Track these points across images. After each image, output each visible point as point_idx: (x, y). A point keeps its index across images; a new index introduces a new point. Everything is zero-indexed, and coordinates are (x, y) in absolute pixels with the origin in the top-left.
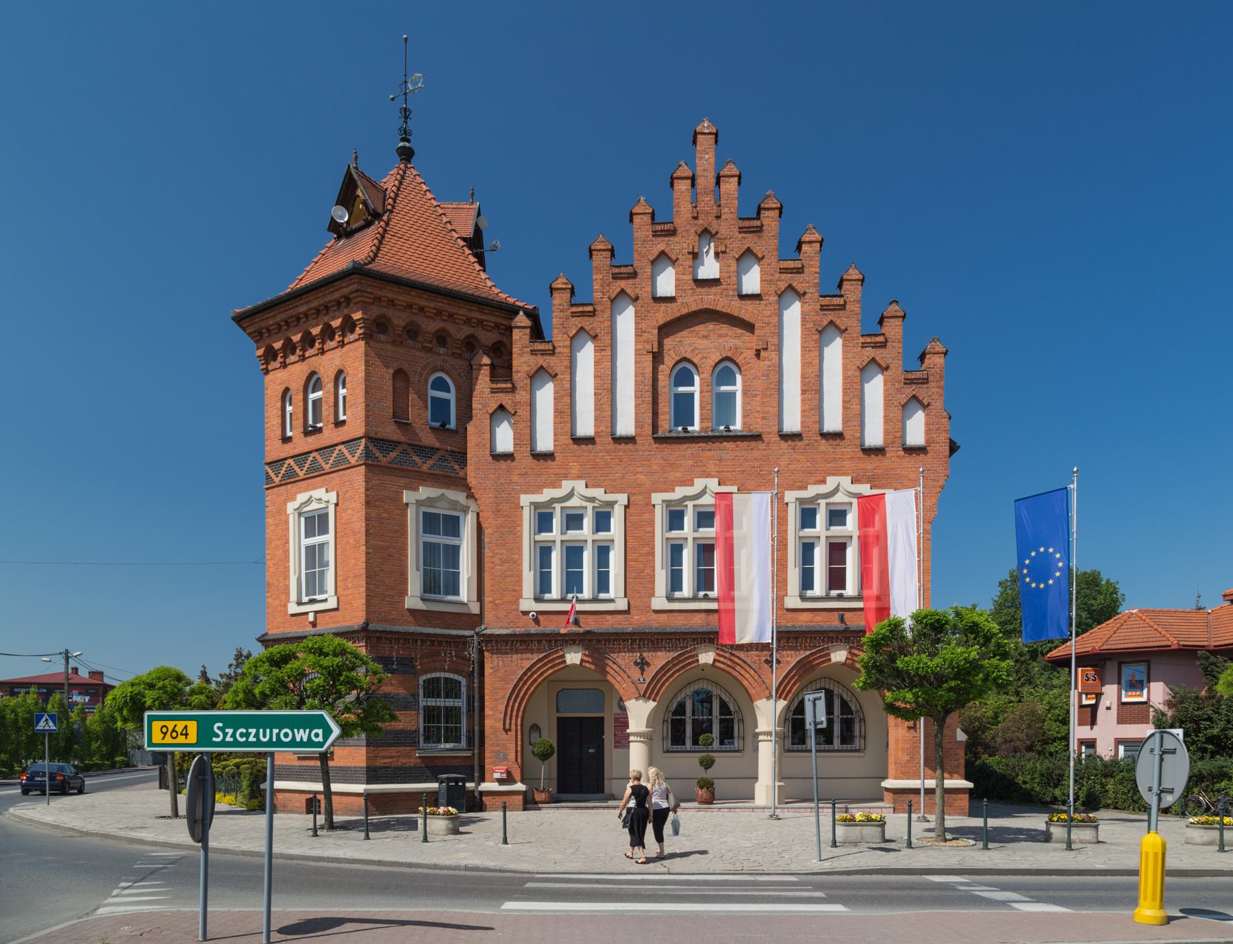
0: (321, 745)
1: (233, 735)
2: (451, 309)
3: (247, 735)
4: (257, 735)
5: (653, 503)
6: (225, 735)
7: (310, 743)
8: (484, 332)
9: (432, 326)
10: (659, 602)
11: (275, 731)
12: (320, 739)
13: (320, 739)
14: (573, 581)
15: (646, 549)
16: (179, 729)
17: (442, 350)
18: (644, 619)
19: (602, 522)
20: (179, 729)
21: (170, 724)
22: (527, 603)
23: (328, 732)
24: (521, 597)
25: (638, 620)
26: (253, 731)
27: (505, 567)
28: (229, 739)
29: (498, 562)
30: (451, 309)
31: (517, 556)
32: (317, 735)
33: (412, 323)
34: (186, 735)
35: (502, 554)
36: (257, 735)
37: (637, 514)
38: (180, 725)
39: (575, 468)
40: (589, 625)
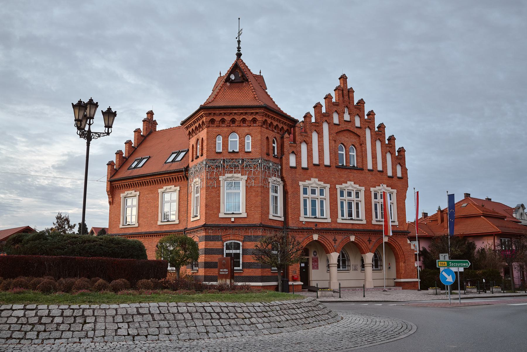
0: (468, 266)
1: (453, 265)
2: (280, 119)
3: (455, 264)
4: (457, 265)
5: (337, 188)
6: (452, 264)
7: (466, 266)
8: (285, 126)
9: (275, 123)
10: (339, 220)
11: (460, 264)
12: (467, 265)
13: (467, 265)
14: (314, 212)
15: (335, 203)
16: (444, 263)
17: (276, 131)
18: (335, 226)
19: (322, 193)
20: (444, 263)
21: (442, 262)
22: (302, 219)
23: (469, 264)
24: (300, 216)
25: (334, 226)
26: (456, 264)
27: (295, 206)
28: (452, 265)
29: (293, 204)
30: (280, 119)
31: (298, 202)
32: (467, 265)
33: (271, 123)
34: (445, 264)
35: (294, 201)
36: (457, 265)
37: (333, 191)
38: (444, 263)
39: (314, 175)
40: (320, 227)
